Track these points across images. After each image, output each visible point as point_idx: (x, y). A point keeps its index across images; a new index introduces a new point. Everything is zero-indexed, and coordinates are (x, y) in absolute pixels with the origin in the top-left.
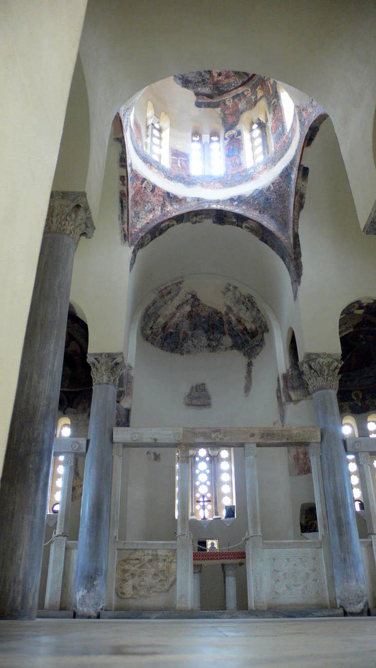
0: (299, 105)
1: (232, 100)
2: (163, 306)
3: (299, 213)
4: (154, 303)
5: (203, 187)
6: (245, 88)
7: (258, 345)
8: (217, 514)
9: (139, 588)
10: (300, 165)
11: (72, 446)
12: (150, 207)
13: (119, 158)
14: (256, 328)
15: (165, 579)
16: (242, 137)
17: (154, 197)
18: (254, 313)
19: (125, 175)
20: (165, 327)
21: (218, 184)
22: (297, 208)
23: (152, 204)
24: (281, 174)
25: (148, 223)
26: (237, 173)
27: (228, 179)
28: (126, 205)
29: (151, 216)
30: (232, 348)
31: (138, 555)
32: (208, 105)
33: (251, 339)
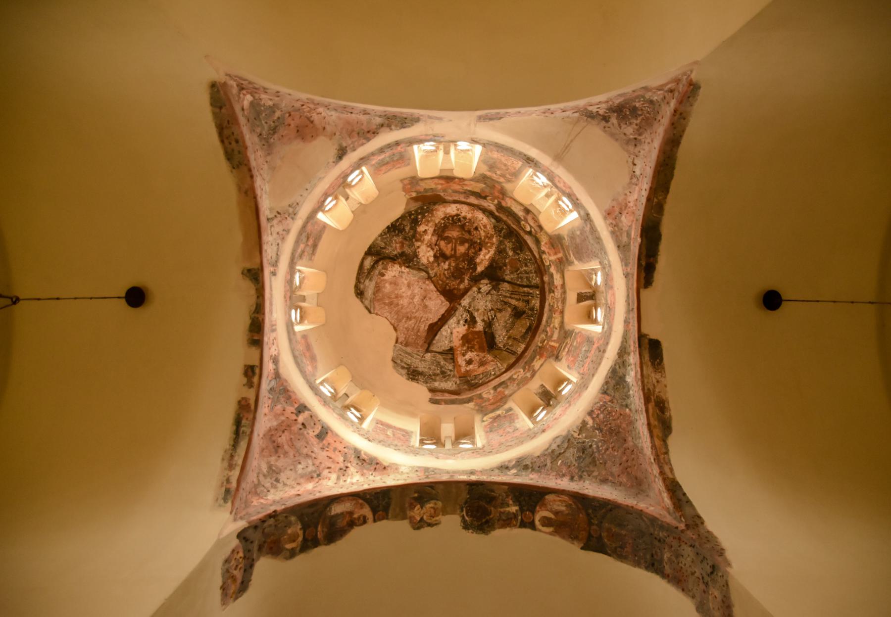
1: (492, 392)
10: (641, 337)
12: (311, 468)
13: (248, 322)
17: (323, 449)
19: (257, 363)
22: (657, 432)
23: (317, 462)
28: (248, 431)
29: (310, 486)
32: (453, 402)
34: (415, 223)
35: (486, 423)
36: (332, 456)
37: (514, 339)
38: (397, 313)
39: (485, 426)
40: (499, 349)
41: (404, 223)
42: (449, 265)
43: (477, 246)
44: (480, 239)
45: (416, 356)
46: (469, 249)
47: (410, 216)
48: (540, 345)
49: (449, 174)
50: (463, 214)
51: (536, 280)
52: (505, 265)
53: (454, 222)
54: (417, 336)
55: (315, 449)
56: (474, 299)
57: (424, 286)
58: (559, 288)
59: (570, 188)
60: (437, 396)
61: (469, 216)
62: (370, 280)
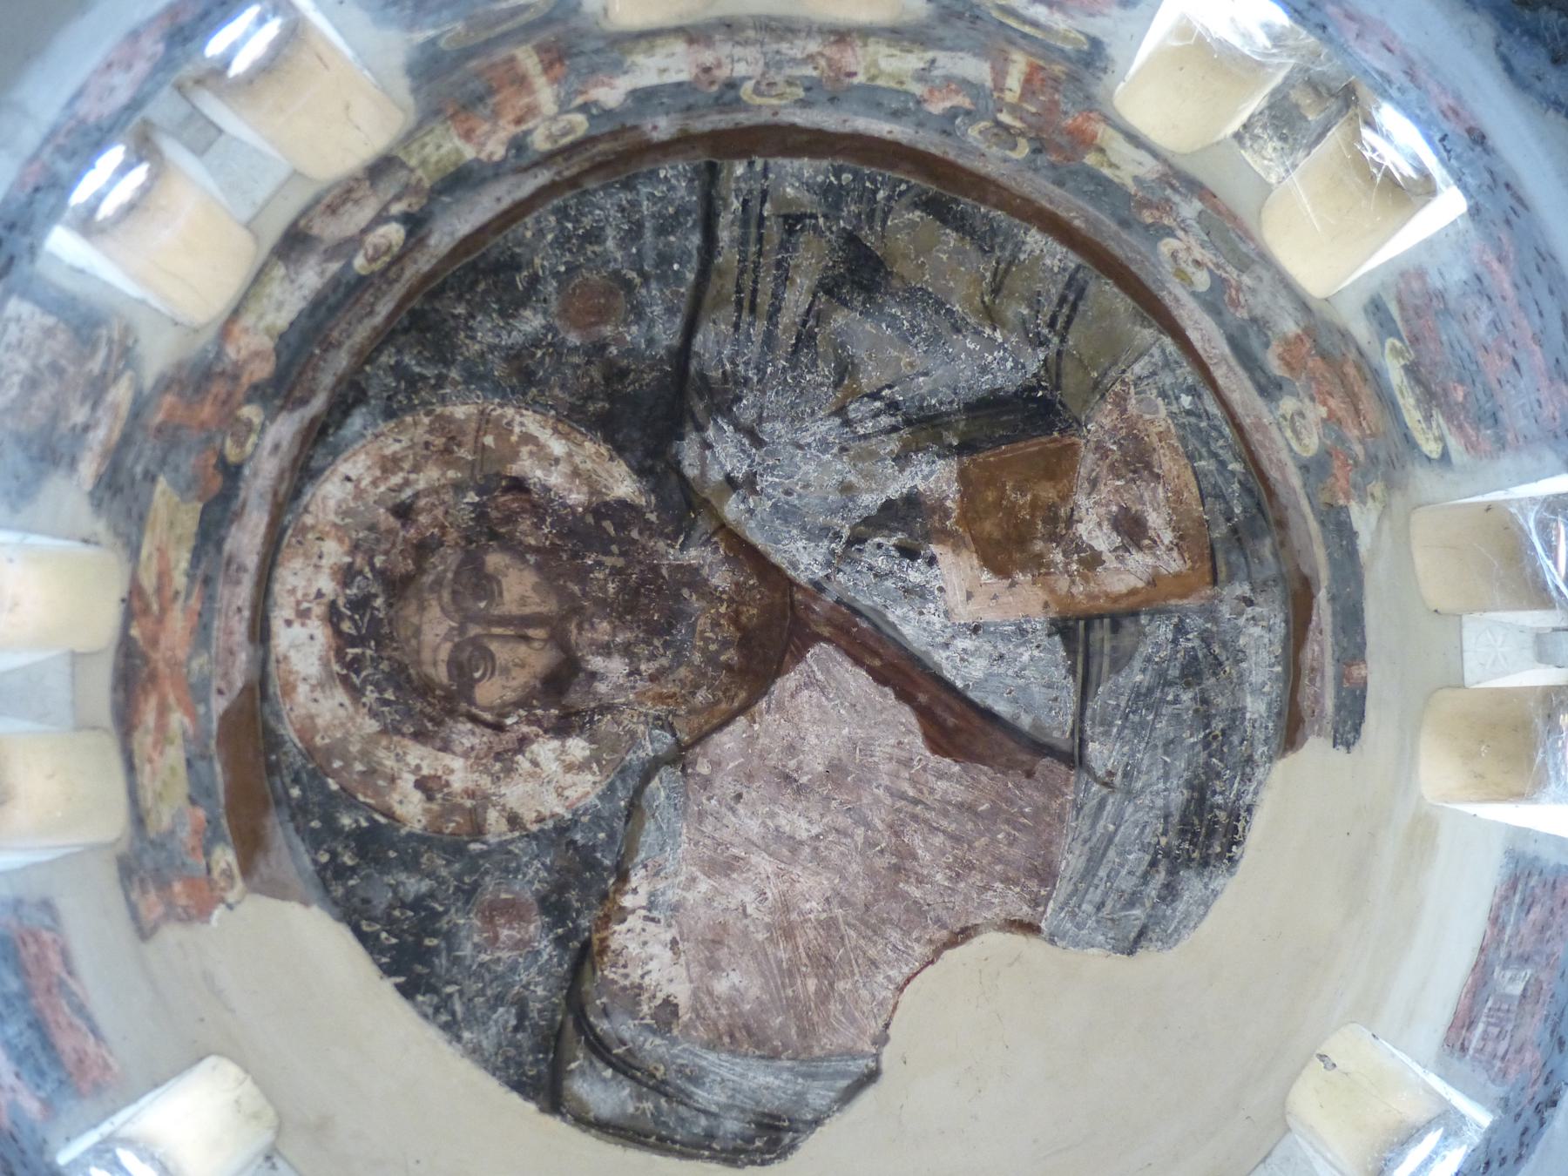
1: (1288, 405)
32: (1351, 619)
34: (378, 843)
35: (1455, 444)
37: (996, 291)
38: (873, 928)
39: (1471, 446)
40: (1053, 368)
41: (382, 900)
42: (606, 650)
43: (503, 502)
44: (458, 488)
45: (1105, 824)
46: (518, 551)
47: (341, 872)
48: (1023, 150)
49: (101, 679)
50: (327, 585)
51: (675, 181)
52: (600, 347)
53: (377, 634)
54: (994, 812)
56: (786, 514)
57: (726, 785)
58: (708, 57)
59: (134, 36)
60: (1322, 703)
61: (334, 552)
62: (696, 1079)
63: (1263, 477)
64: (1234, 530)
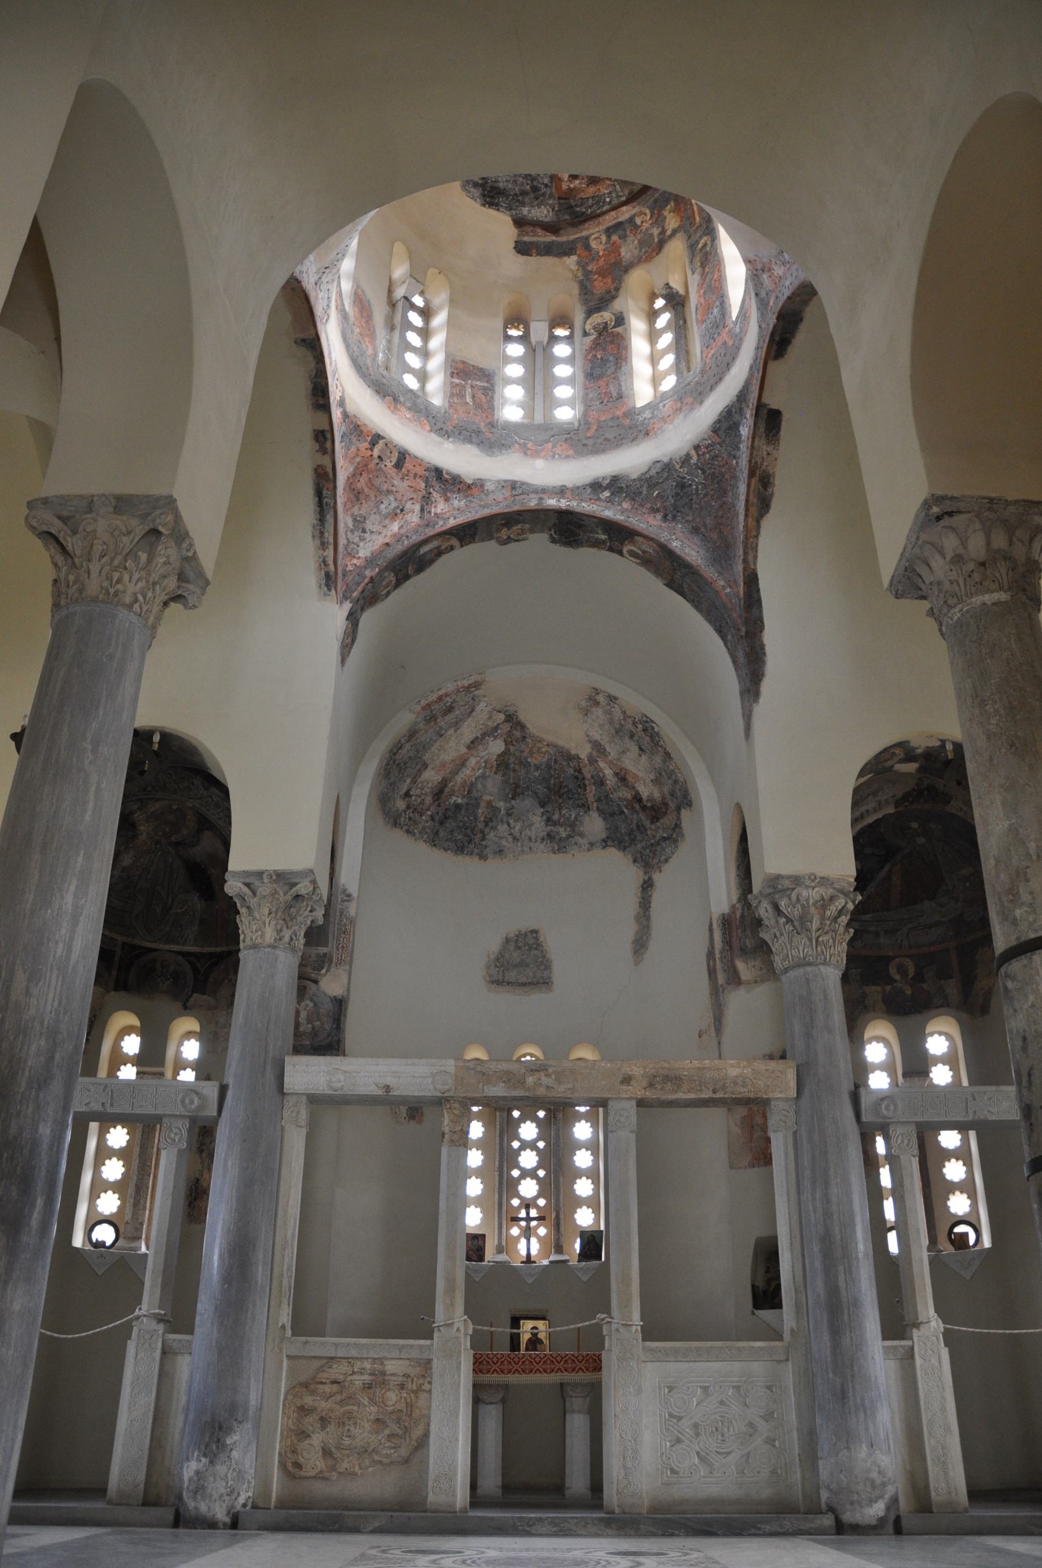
0: (751, 256)
1: (604, 238)
2: (436, 741)
3: (758, 522)
4: (412, 734)
5: (526, 454)
6: (636, 210)
7: (665, 839)
8: (559, 1249)
9: (337, 1454)
10: (760, 406)
11: (183, 1101)
12: (394, 504)
13: (310, 386)
14: (664, 798)
15: (400, 1432)
16: (626, 329)
17: (402, 479)
18: (658, 759)
19: (327, 428)
20: (441, 791)
21: (565, 446)
22: (754, 510)
24: (715, 423)
25: (387, 544)
26: (612, 419)
27: (589, 435)
29: (395, 527)
30: (605, 843)
31: (337, 1371)
32: (547, 250)
33: (652, 823)
36: (414, 485)
55: (395, 482)
63: (585, 221)
64: (572, 207)
